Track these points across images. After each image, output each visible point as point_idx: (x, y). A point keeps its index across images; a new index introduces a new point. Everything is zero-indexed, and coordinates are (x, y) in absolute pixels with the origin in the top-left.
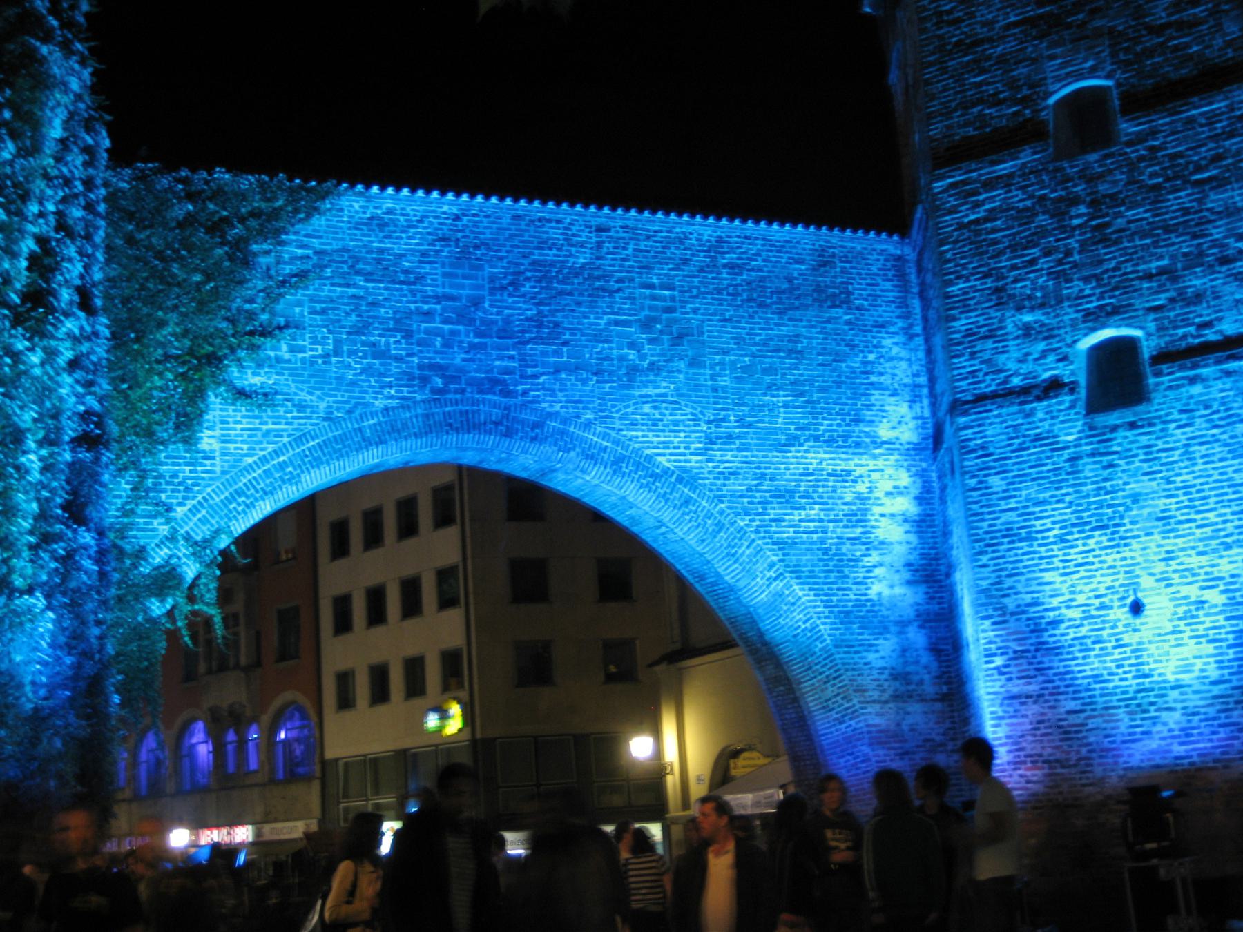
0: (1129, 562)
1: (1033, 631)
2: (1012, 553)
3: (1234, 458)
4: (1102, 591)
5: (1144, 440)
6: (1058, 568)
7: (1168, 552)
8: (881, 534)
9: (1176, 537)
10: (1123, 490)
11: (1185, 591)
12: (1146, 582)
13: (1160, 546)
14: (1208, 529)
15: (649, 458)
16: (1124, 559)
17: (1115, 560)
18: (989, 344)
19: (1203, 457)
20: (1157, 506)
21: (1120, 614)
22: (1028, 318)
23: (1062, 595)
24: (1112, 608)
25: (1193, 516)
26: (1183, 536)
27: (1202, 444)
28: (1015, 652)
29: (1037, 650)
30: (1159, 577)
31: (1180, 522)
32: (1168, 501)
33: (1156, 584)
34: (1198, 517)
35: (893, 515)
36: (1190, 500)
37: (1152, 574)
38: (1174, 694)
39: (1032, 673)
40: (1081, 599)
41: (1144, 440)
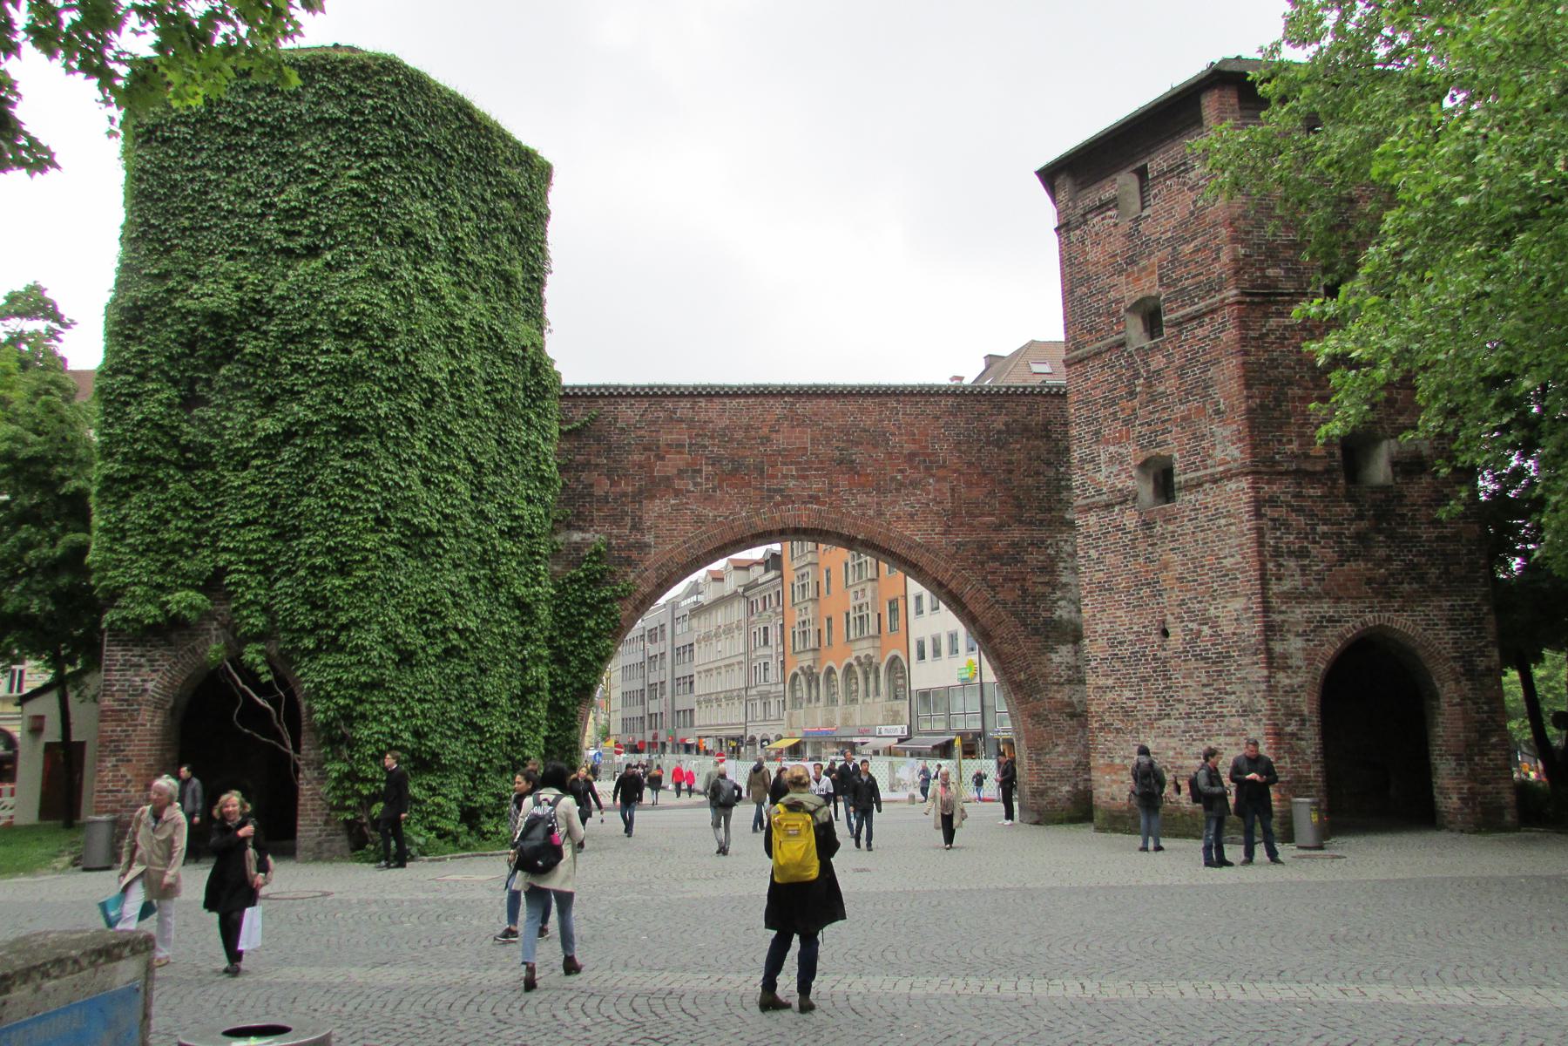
5: (1170, 528)
8: (1064, 580)
11: (1191, 625)
12: (1170, 618)
15: (909, 538)
18: (1091, 466)
21: (1155, 638)
22: (1112, 449)
38: (1182, 692)
41: (1170, 528)
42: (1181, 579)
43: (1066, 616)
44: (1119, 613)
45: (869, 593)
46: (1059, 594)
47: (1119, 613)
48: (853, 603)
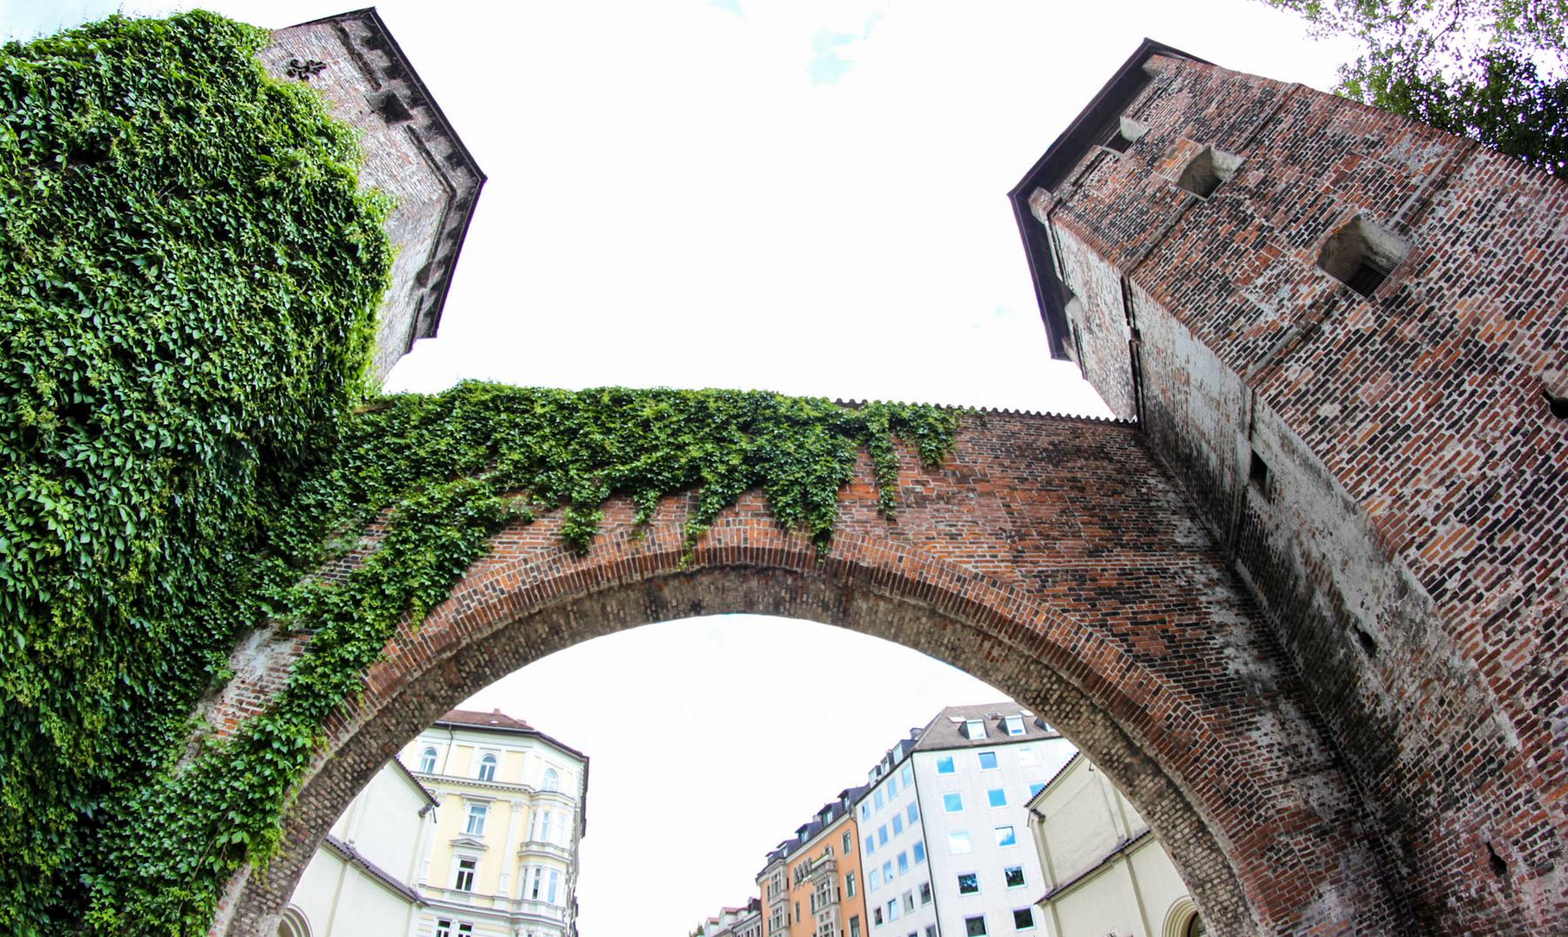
0: (1518, 373)
1: (1472, 522)
2: (1392, 459)
3: (1519, 226)
4: (1515, 422)
5: (1435, 274)
6: (1452, 437)
7: (1544, 336)
9: (1538, 319)
10: (1456, 321)
13: (1531, 338)
14: (1559, 289)
16: (1510, 376)
17: (1502, 384)
19: (1495, 245)
20: (1496, 309)
23: (1477, 458)
24: (1539, 429)
25: (1536, 291)
26: (1545, 312)
27: (1484, 239)
28: (1465, 561)
29: (1490, 540)
30: (1557, 363)
31: (1530, 304)
32: (1502, 298)
33: (1561, 372)
34: (1540, 287)
35: (1218, 602)
36: (1520, 282)
37: (1550, 366)
39: (1502, 569)
40: (1500, 448)
41: (1435, 274)
42: (1514, 313)
43: (1243, 670)
44: (1448, 454)
45: (833, 914)
46: (1219, 640)
47: (1448, 454)
48: (819, 924)
